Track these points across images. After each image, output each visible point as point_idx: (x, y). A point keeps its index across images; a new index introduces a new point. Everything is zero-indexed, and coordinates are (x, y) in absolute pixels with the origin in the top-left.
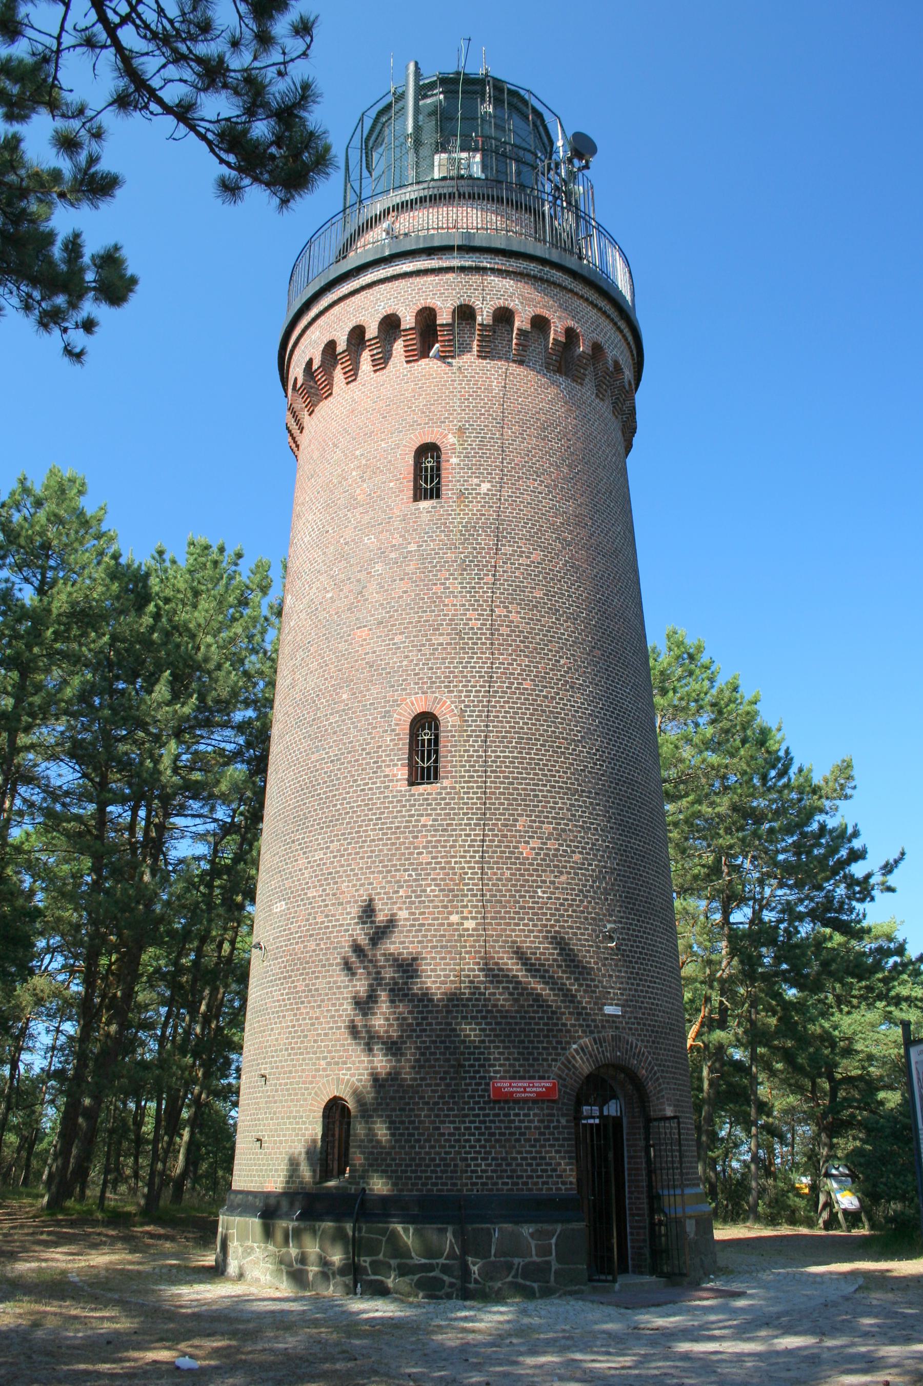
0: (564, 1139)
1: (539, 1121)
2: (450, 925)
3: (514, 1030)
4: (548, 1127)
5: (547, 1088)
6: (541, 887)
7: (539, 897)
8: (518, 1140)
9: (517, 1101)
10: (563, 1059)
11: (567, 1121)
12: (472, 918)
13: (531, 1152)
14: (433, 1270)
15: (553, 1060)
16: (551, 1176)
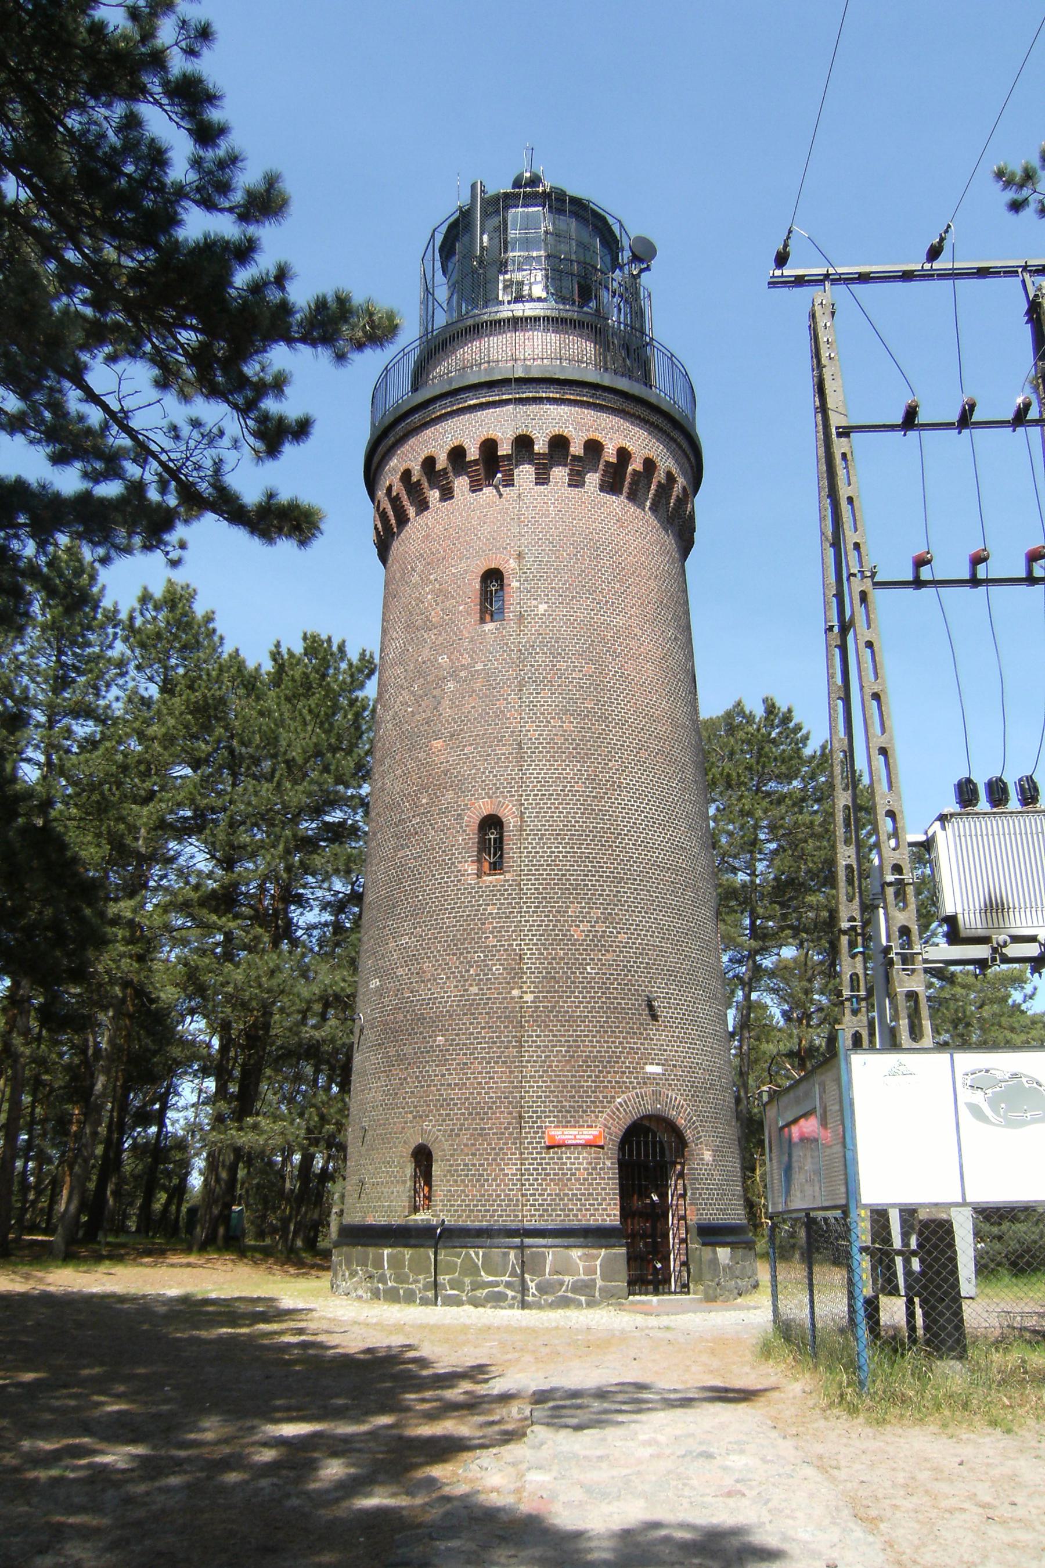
2: (512, 998)
3: (565, 1087)
4: (595, 1169)
8: (569, 1180)
9: (568, 1146)
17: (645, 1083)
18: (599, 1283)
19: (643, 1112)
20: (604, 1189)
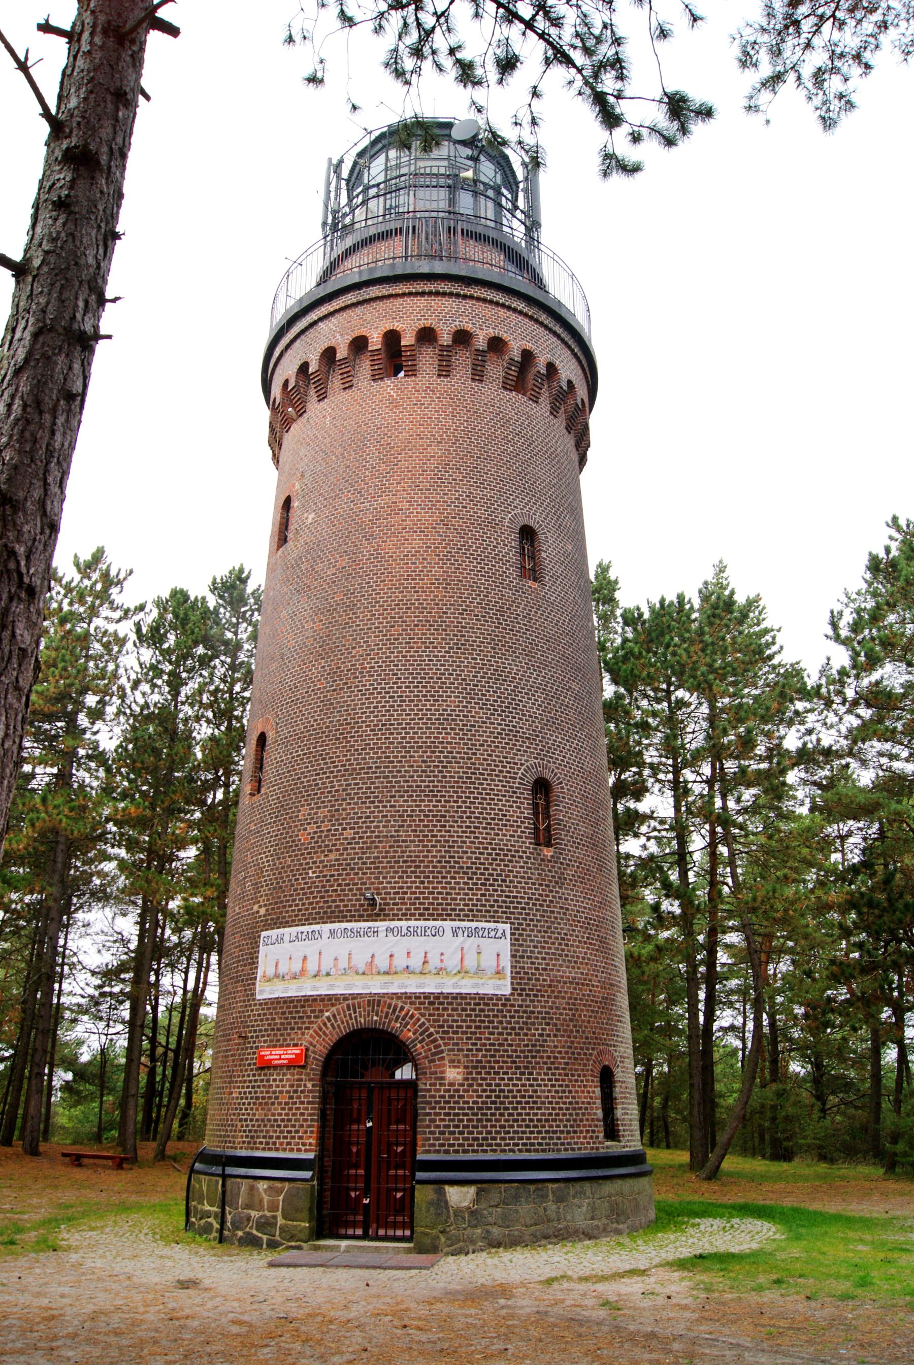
0: (309, 1103)
4: (296, 1091)
6: (311, 868)
9: (275, 1067)
10: (315, 1026)
12: (265, 905)
18: (280, 1221)
19: (353, 1025)
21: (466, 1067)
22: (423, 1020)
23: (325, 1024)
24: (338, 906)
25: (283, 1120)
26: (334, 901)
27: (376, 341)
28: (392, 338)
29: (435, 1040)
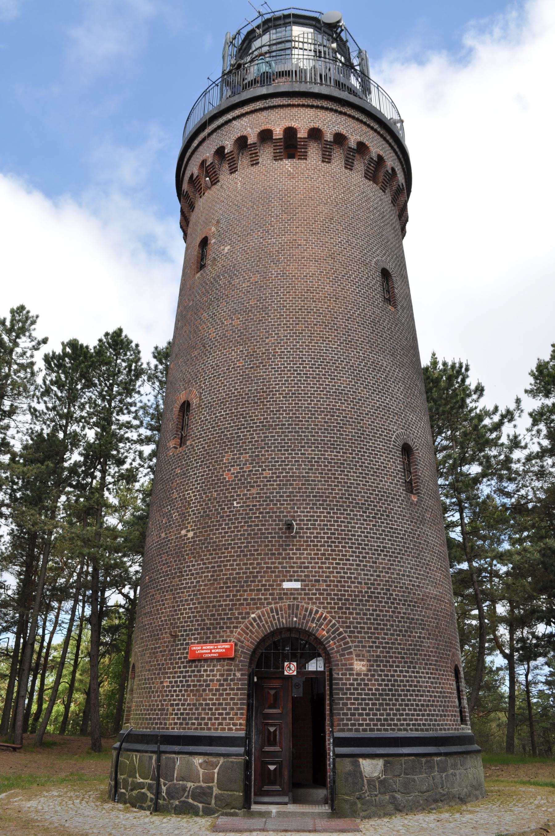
0: (238, 689)
1: (220, 675)
2: (181, 537)
4: (226, 680)
5: (226, 649)
6: (236, 500)
7: (234, 507)
8: (204, 690)
9: (206, 660)
10: (242, 626)
11: (242, 675)
12: (193, 530)
13: (212, 699)
14: (143, 789)
15: (234, 627)
16: (225, 719)
17: (281, 599)
18: (216, 791)
19: (276, 625)
20: (232, 699)
21: (369, 661)
22: (334, 621)
23: (251, 624)
24: (261, 530)
25: (214, 704)
26: (257, 525)
27: (278, 132)
28: (290, 132)
29: (344, 638)
